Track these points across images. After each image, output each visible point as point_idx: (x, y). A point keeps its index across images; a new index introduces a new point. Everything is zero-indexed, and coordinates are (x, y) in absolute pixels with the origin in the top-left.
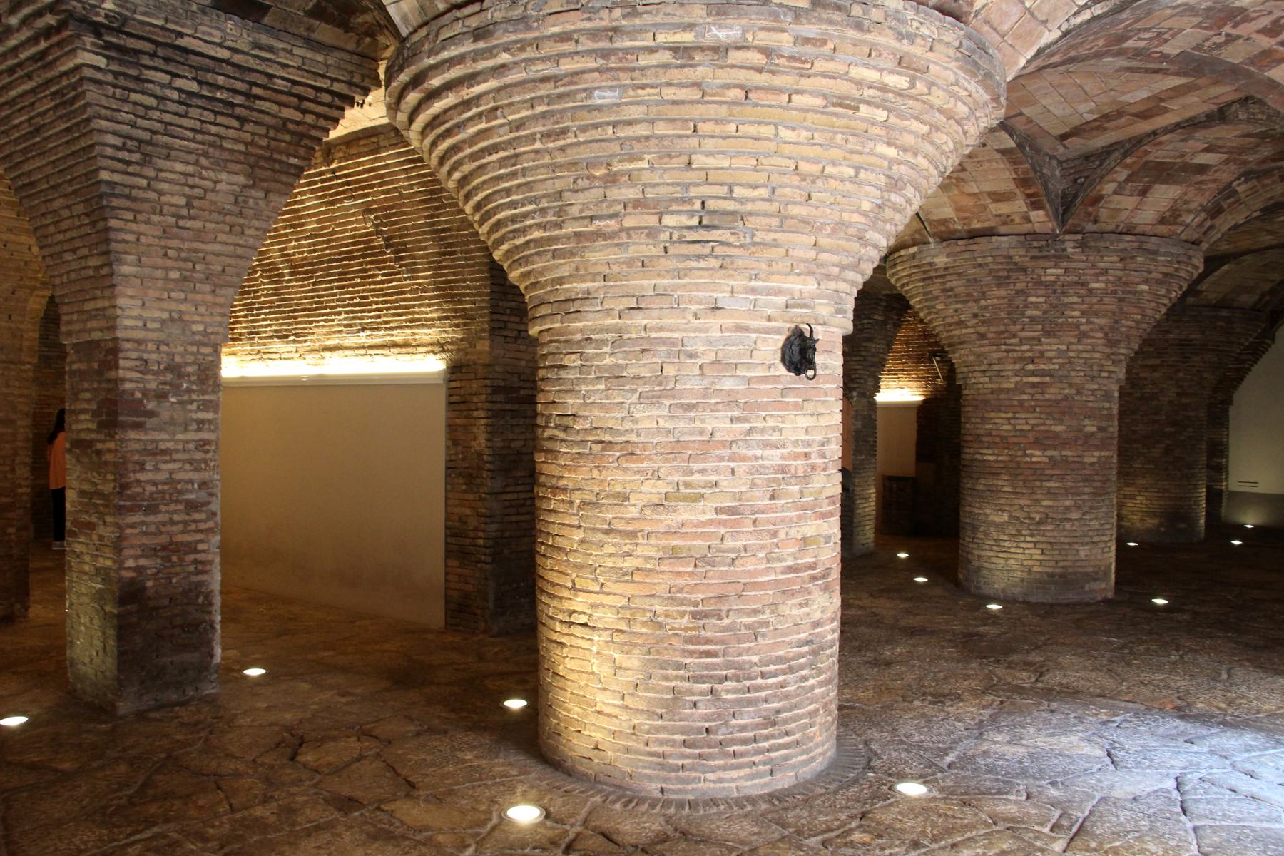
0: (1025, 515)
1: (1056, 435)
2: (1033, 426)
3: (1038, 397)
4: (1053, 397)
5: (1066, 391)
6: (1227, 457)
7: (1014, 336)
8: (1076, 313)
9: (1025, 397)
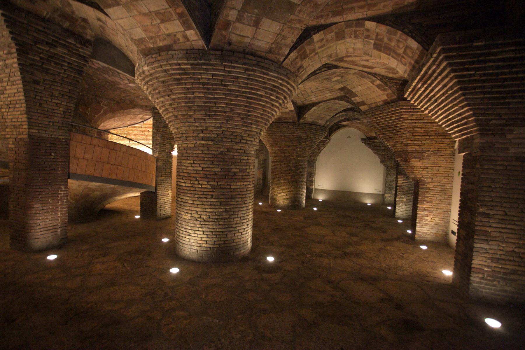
0: (199, 216)
2: (203, 168)
5: (222, 150)
6: (315, 178)
9: (199, 152)
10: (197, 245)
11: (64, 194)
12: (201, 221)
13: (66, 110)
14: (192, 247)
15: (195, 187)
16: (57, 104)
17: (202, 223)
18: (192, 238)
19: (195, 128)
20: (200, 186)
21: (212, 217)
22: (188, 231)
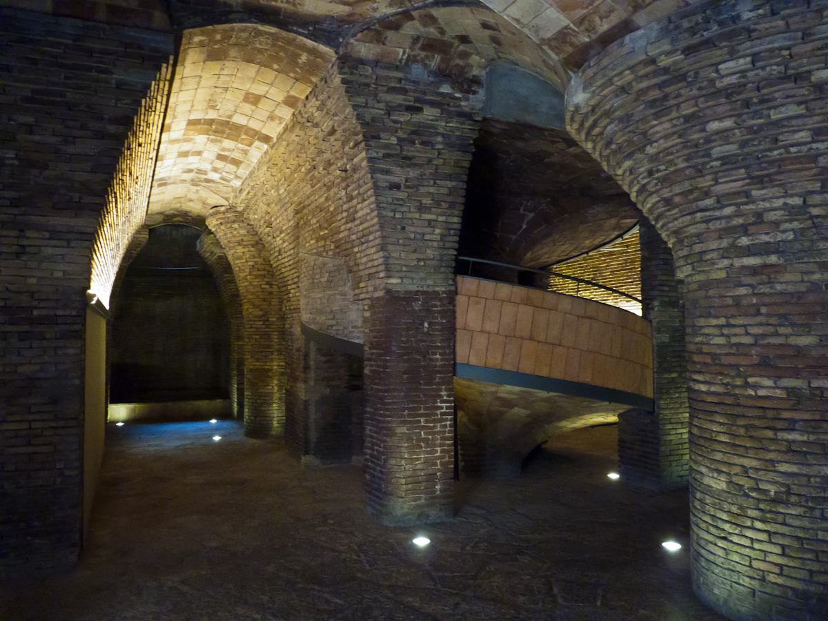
0: (751, 483)
1: (799, 351)
2: (756, 336)
3: (765, 289)
4: (790, 288)
5: (816, 277)
7: (706, 194)
8: (803, 136)
9: (742, 291)
10: (751, 573)
11: (447, 408)
12: (758, 500)
13: (445, 232)
14: (735, 578)
15: (735, 395)
16: (430, 221)
17: (762, 506)
18: (735, 548)
19: (723, 224)
20: (753, 393)
21: (795, 489)
22: (720, 524)
